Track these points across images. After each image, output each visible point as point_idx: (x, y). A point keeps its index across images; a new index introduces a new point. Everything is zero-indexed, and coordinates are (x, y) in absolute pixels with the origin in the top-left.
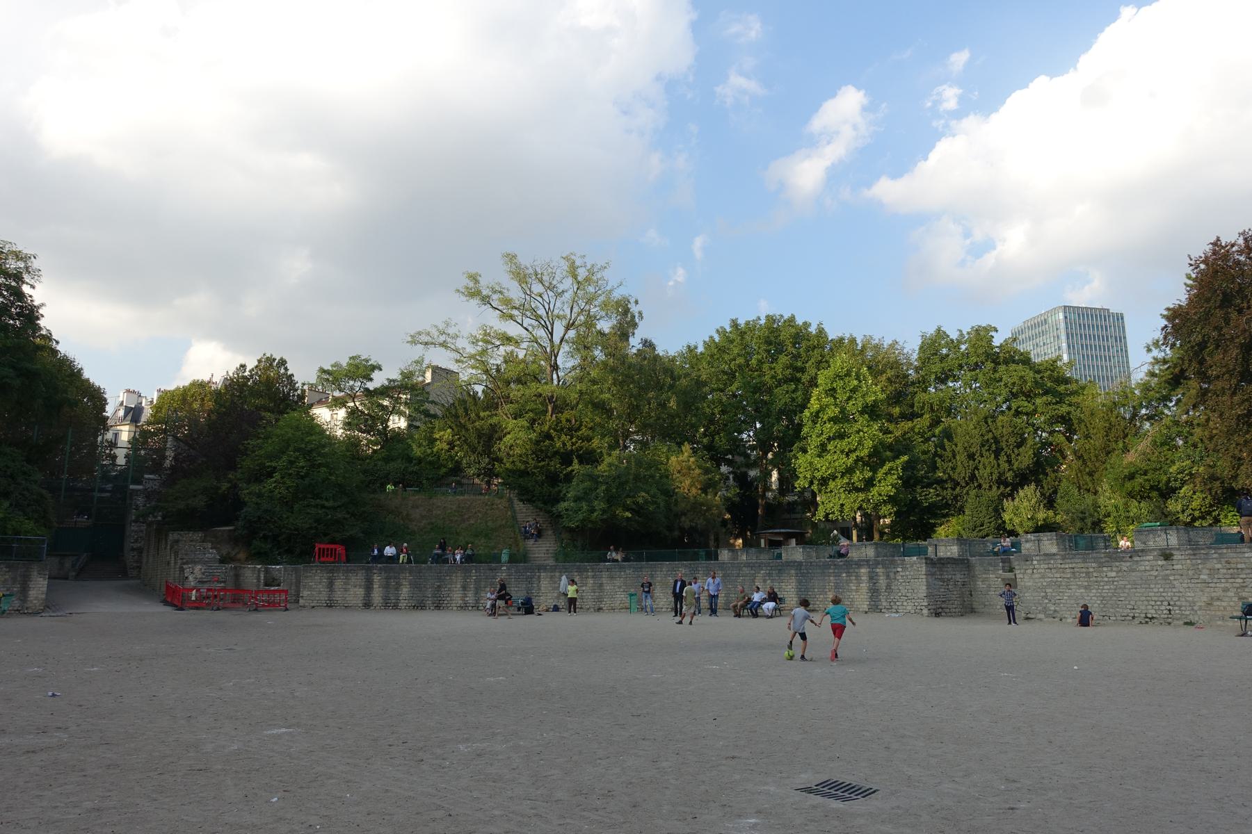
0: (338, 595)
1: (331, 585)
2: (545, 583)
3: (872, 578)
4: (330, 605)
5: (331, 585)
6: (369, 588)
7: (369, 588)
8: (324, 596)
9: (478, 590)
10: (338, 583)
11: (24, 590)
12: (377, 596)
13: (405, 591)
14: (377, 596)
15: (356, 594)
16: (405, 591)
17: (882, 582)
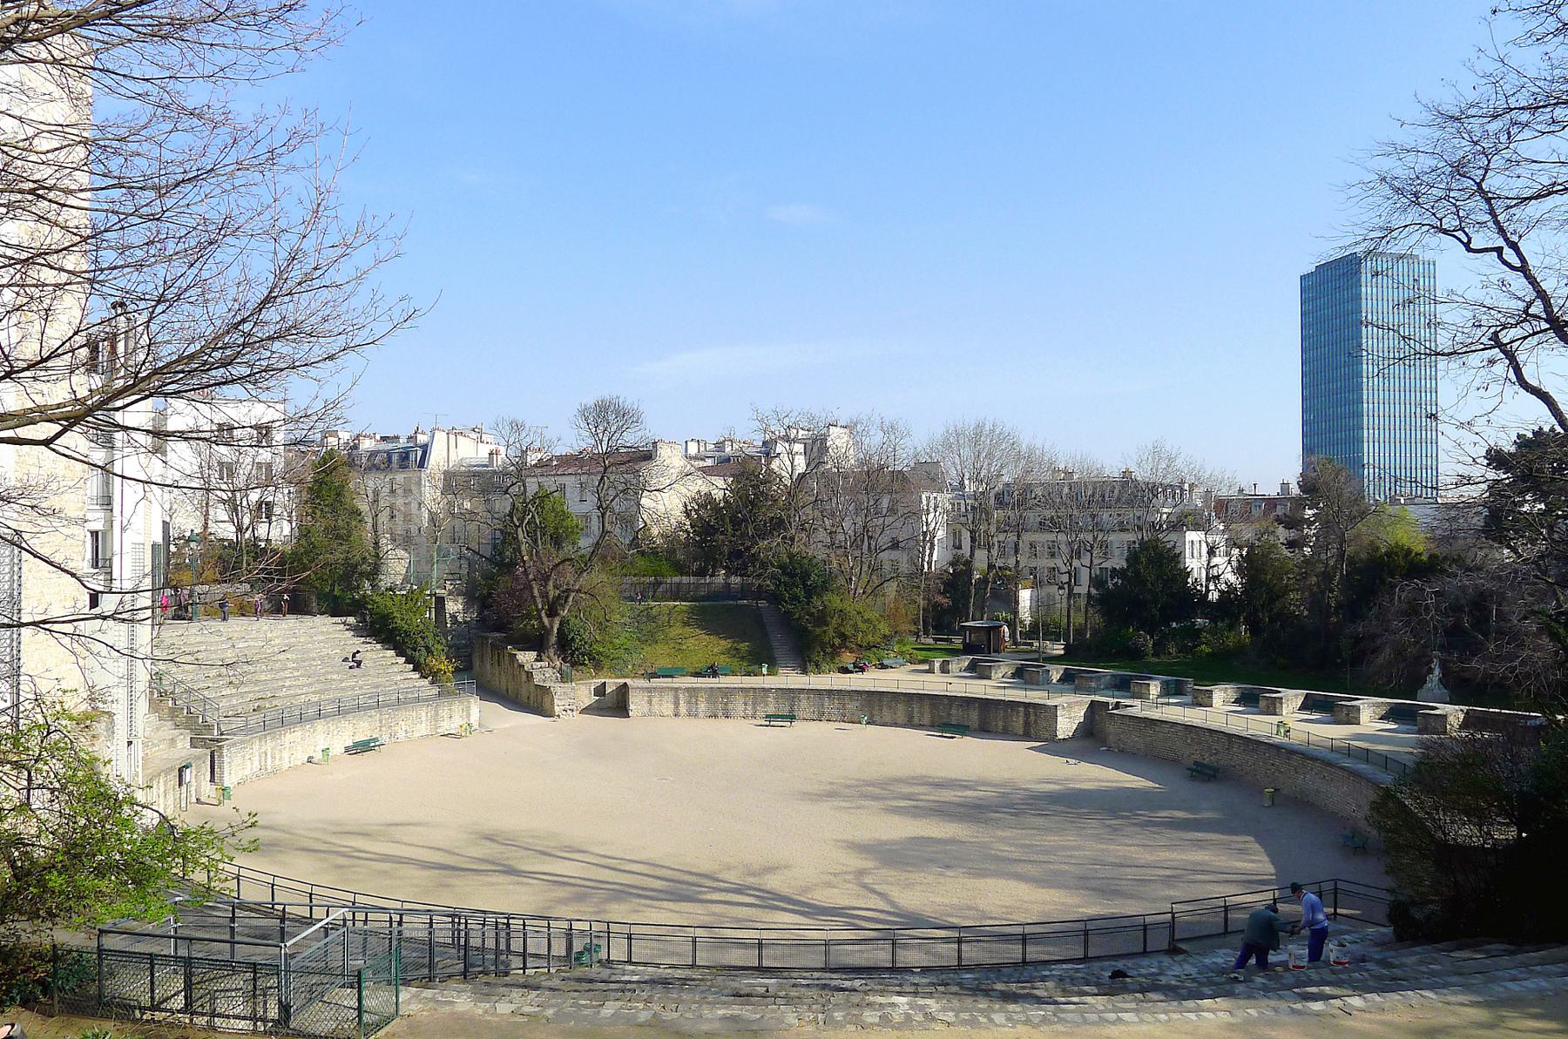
0: (656, 708)
1: (650, 703)
2: (804, 703)
3: (1027, 715)
4: (651, 714)
5: (650, 703)
6: (677, 704)
7: (677, 704)
8: (646, 710)
9: (754, 708)
10: (655, 700)
11: (468, 716)
12: (683, 709)
13: (702, 706)
14: (683, 709)
15: (668, 708)
16: (702, 706)
17: (1032, 718)
